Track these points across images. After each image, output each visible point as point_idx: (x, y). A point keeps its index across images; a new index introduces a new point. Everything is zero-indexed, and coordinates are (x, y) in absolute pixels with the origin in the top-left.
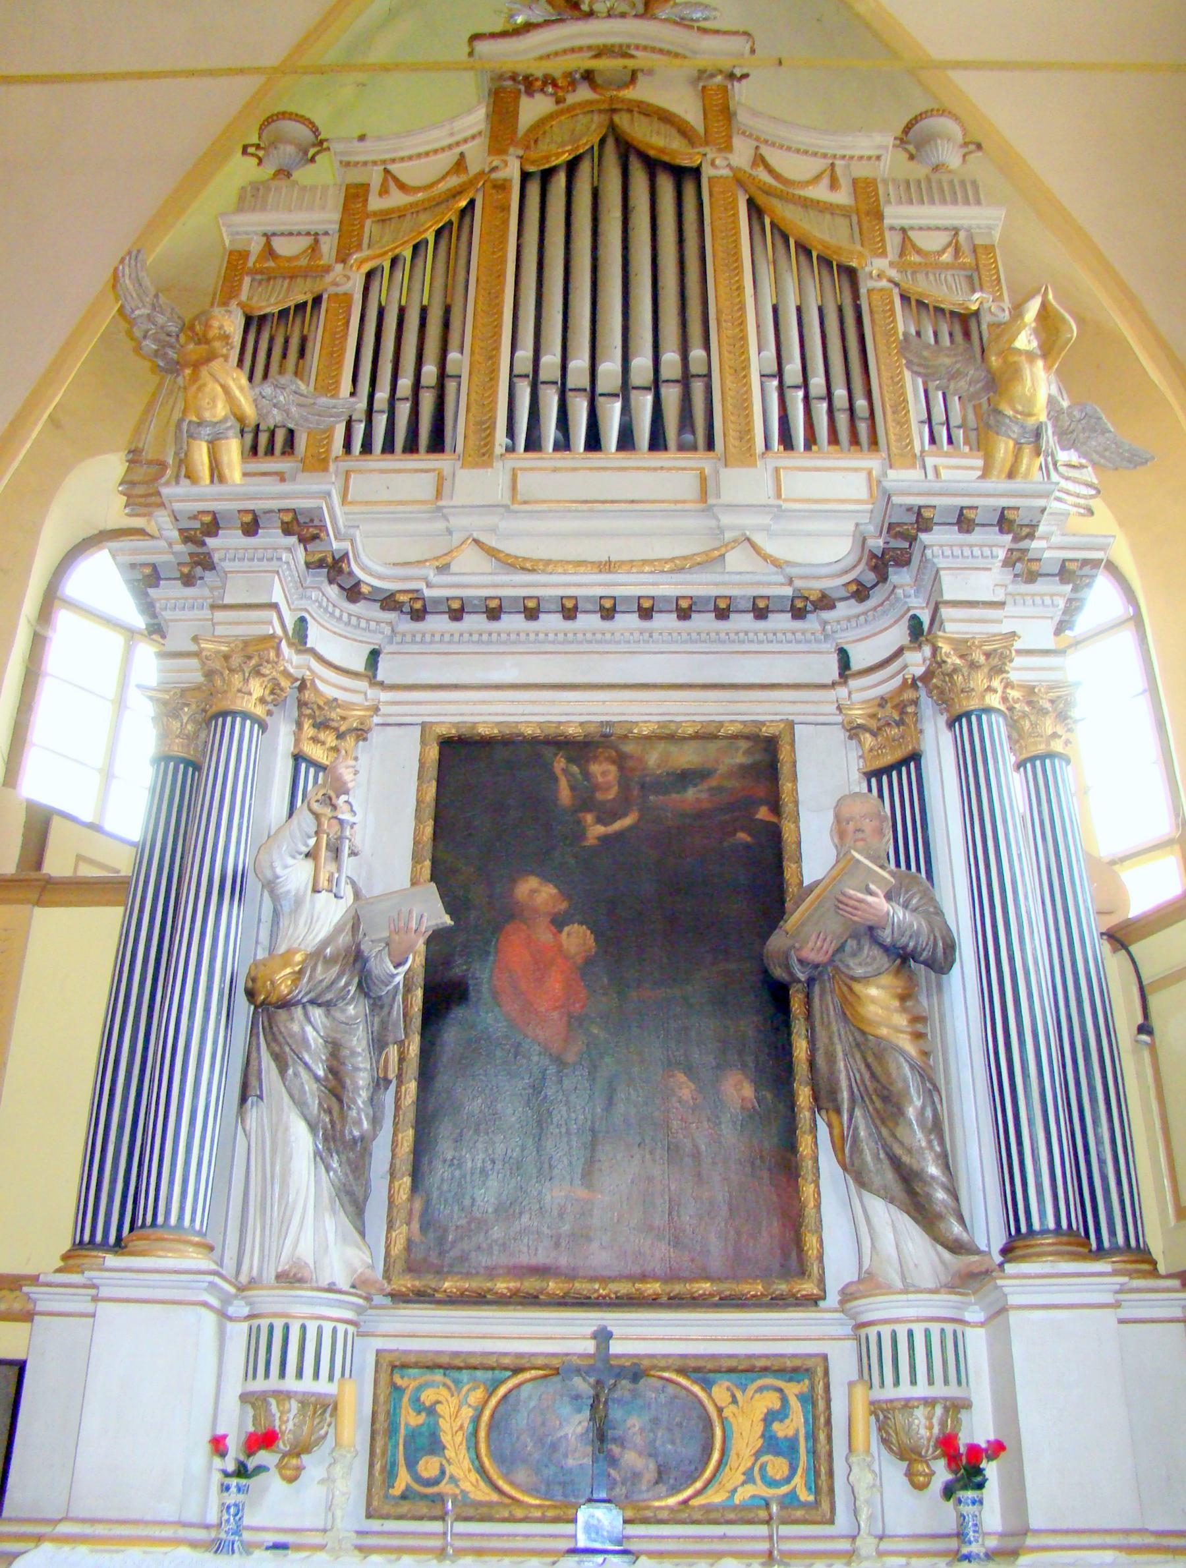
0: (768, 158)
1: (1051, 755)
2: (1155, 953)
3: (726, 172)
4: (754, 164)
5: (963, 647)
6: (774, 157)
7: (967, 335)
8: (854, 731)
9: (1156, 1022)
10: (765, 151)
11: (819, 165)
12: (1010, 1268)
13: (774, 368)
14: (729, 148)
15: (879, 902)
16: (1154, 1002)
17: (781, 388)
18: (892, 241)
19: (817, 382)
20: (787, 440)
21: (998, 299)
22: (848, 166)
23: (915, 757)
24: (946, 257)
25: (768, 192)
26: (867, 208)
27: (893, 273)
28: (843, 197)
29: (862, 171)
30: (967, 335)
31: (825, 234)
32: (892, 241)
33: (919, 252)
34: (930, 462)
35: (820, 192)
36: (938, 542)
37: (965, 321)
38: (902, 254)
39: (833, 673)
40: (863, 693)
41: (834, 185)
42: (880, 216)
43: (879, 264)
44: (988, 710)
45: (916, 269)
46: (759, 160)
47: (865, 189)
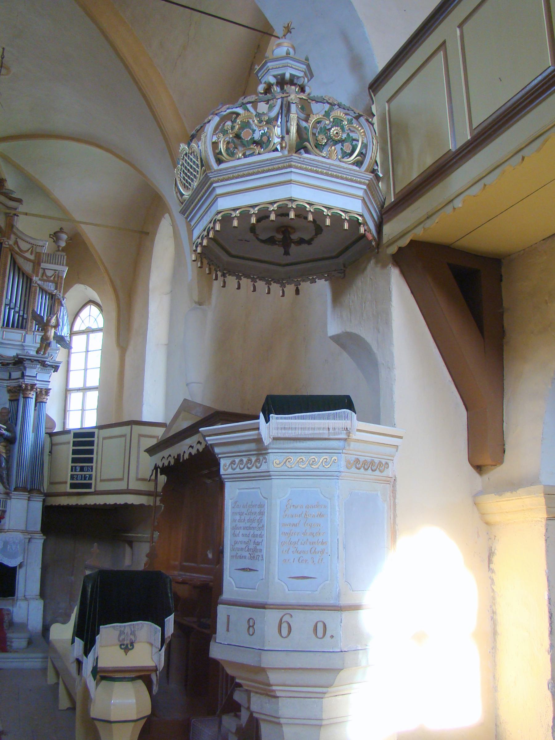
0: (19, 243)
1: (43, 402)
2: (57, 439)
3: (7, 246)
4: (15, 244)
5: (27, 385)
6: (21, 243)
7: (52, 298)
8: (9, 391)
9: (53, 452)
10: (18, 240)
11: (29, 246)
12: (13, 493)
13: (9, 303)
14: (9, 238)
15: (4, 432)
16: (54, 448)
17: (9, 308)
18: (41, 271)
19: (17, 309)
20: (8, 325)
21: (60, 292)
22: (36, 248)
23: (18, 400)
24: (52, 278)
25: (17, 253)
26: (37, 263)
27: (39, 282)
28: (32, 257)
29: (38, 250)
30: (52, 298)
31: (28, 268)
32: (41, 271)
33: (46, 276)
34: (35, 333)
35: (28, 255)
36: (27, 363)
37: (52, 297)
38: (42, 277)
39: (7, 378)
40: (13, 384)
41: (31, 254)
42: (40, 265)
43: (37, 279)
44: (29, 398)
45: (45, 281)
46: (16, 243)
47: (38, 255)
